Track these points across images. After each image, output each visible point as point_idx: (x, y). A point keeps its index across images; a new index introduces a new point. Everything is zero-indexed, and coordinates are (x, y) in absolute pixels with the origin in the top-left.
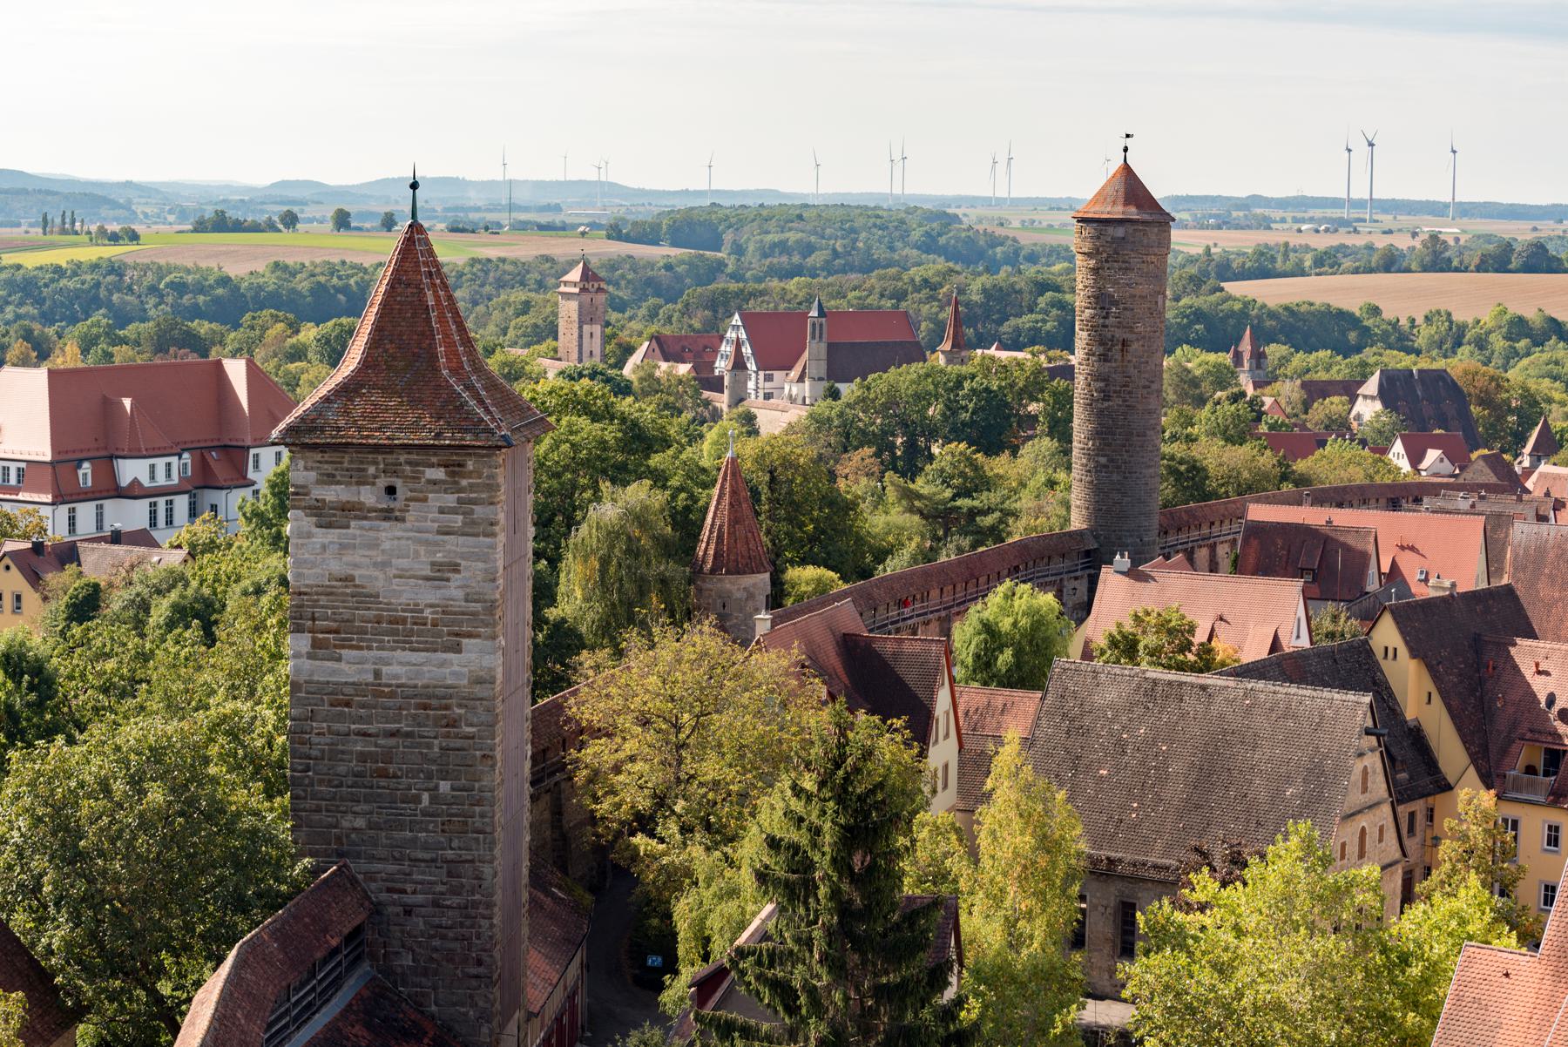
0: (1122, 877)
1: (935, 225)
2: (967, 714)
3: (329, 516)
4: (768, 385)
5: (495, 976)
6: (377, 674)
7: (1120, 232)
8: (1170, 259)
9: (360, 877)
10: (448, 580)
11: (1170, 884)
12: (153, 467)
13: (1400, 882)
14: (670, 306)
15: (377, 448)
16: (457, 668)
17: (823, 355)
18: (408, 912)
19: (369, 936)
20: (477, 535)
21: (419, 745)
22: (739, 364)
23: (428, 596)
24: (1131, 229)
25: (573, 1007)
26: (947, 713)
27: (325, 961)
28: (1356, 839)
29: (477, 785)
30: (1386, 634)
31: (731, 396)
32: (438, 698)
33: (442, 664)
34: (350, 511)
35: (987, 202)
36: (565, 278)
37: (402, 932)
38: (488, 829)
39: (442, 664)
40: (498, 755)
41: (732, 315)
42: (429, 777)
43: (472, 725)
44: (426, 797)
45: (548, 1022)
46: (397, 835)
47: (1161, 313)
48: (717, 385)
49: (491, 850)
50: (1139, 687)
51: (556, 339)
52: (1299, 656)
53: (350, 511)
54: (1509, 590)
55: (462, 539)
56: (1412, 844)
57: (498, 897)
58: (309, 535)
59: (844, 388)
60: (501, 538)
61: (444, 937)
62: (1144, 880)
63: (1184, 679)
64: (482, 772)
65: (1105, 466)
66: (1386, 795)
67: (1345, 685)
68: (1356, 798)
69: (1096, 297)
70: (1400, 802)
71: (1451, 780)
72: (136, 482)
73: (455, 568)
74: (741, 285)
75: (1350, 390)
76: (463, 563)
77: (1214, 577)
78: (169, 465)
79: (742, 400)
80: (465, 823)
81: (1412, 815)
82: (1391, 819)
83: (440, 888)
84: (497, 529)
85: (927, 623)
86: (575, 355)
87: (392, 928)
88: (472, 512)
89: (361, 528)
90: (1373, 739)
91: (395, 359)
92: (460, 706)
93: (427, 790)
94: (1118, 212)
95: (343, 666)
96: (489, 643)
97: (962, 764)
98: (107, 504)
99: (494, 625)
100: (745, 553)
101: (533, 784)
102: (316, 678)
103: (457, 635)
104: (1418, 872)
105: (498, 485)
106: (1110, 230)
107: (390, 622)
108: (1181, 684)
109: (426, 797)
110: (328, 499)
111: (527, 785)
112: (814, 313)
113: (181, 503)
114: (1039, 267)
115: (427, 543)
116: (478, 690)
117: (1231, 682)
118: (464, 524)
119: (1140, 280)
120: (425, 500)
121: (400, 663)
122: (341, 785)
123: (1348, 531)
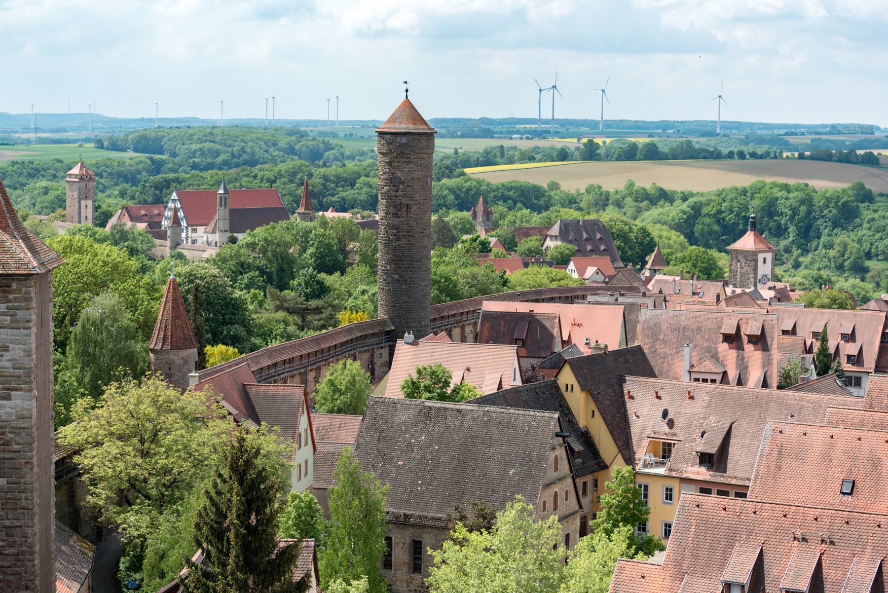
0: (413, 526)
1: (293, 138)
2: (318, 430)
4: (194, 235)
7: (404, 140)
8: (435, 156)
11: (442, 529)
13: (579, 524)
14: (134, 188)
16: (8, 410)
17: (227, 217)
20: (19, 329)
22: (176, 221)
24: (411, 138)
26: (306, 430)
28: (552, 499)
29: (22, 480)
30: (567, 377)
31: (171, 242)
35: (324, 123)
36: (70, 172)
40: (35, 461)
41: (171, 193)
43: (18, 444)
47: (430, 189)
48: (162, 236)
49: (32, 519)
50: (421, 411)
51: (65, 208)
52: (515, 390)
54: (639, 348)
55: (10, 331)
56: (585, 501)
57: (37, 548)
59: (240, 236)
60: (34, 329)
62: (426, 527)
63: (447, 406)
65: (398, 280)
66: (568, 472)
67: (543, 407)
68: (552, 475)
69: (391, 179)
70: (578, 476)
71: (608, 464)
74: (176, 175)
75: (542, 232)
76: (11, 346)
77: (463, 345)
79: (178, 244)
80: (16, 504)
81: (585, 484)
82: (572, 486)
84: (31, 324)
85: (292, 376)
86: (77, 219)
88: (15, 315)
90: (561, 439)
92: (11, 433)
94: (402, 127)
96: (27, 394)
97: (315, 461)
99: (30, 383)
100: (181, 335)
101: (56, 479)
103: (8, 389)
104: (589, 517)
106: (398, 139)
108: (445, 409)
111: (53, 480)
112: (221, 191)
114: (356, 162)
116: (22, 424)
117: (475, 407)
118: (11, 321)
119: (416, 168)
123: (543, 315)
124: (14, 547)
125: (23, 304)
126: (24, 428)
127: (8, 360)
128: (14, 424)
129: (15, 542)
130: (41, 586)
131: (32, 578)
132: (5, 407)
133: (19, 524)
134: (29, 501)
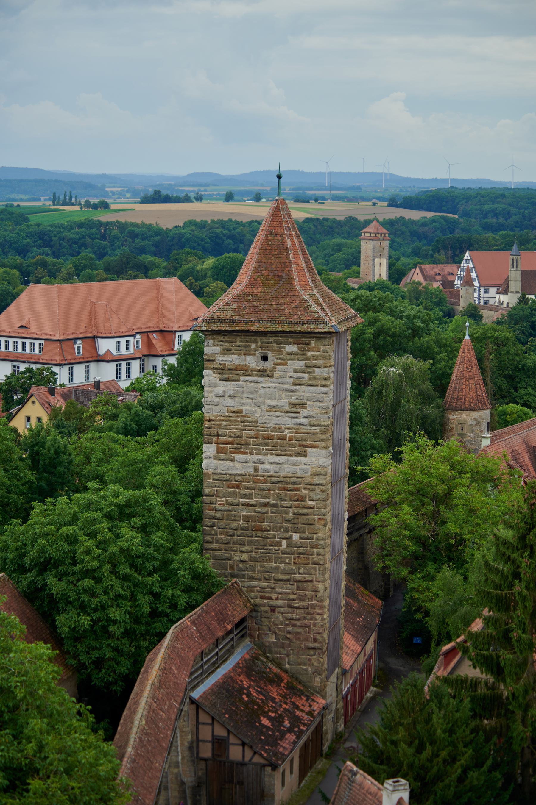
3: (227, 374)
5: (325, 648)
6: (256, 470)
9: (245, 589)
10: (299, 413)
12: (118, 343)
15: (257, 333)
16: (304, 467)
18: (273, 609)
19: (250, 623)
20: (316, 386)
21: (281, 512)
23: (287, 421)
25: (370, 666)
27: (223, 638)
29: (315, 536)
32: (293, 483)
33: (295, 464)
34: (240, 371)
37: (269, 622)
38: (322, 563)
39: (295, 464)
42: (287, 531)
43: (312, 500)
44: (284, 543)
45: (354, 675)
46: (266, 565)
49: (323, 574)
53: (240, 371)
55: (308, 388)
57: (327, 602)
58: (215, 385)
60: (332, 387)
61: (294, 626)
64: (319, 529)
72: (108, 352)
73: (303, 406)
76: (308, 402)
78: (128, 342)
80: (308, 559)
83: (292, 596)
87: (263, 620)
89: (246, 381)
91: (268, 279)
92: (305, 489)
93: (285, 538)
95: (235, 464)
96: (324, 451)
98: (92, 366)
101: (348, 535)
102: (219, 471)
103: (304, 446)
105: (330, 356)
107: (264, 438)
109: (284, 543)
110: (227, 363)
113: (135, 365)
115: (287, 390)
116: (317, 480)
118: (309, 379)
120: (285, 364)
121: (270, 463)
122: (233, 535)
124: (304, 600)
125: (321, 362)
126: (318, 485)
127: (305, 417)
128: (309, 480)
129: (306, 595)
130: (328, 637)
131: (321, 631)
132: (300, 463)
133: (310, 579)
134: (321, 557)
